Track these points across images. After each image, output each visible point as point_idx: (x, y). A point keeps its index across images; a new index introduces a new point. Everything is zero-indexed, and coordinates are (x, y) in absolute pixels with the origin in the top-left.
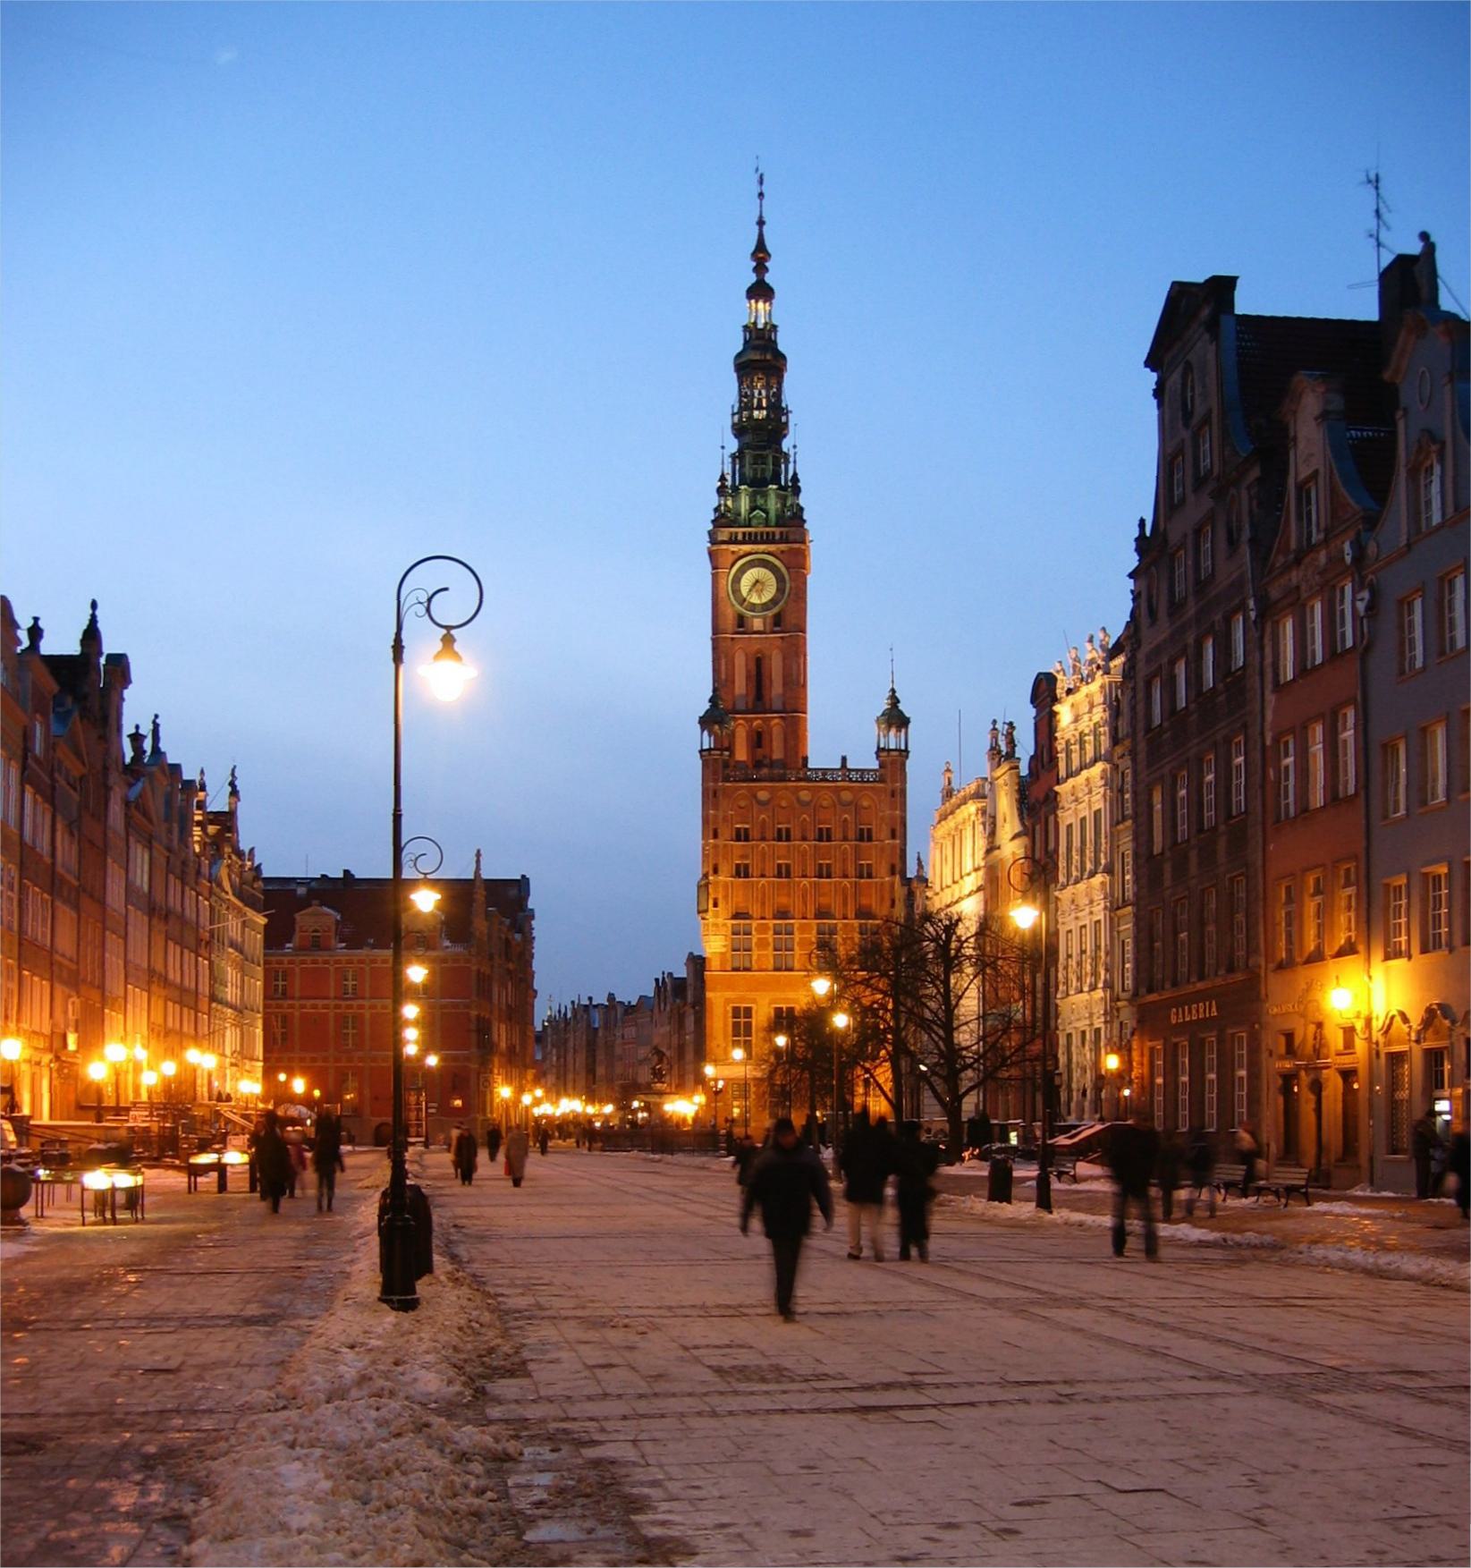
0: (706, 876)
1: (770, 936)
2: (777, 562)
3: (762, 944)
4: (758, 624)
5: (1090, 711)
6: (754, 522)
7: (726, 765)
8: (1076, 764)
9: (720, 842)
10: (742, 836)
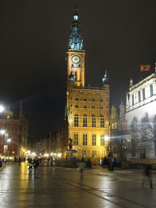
2: (79, 56)
3: (81, 121)
4: (75, 66)
9: (73, 100)
10: (77, 99)
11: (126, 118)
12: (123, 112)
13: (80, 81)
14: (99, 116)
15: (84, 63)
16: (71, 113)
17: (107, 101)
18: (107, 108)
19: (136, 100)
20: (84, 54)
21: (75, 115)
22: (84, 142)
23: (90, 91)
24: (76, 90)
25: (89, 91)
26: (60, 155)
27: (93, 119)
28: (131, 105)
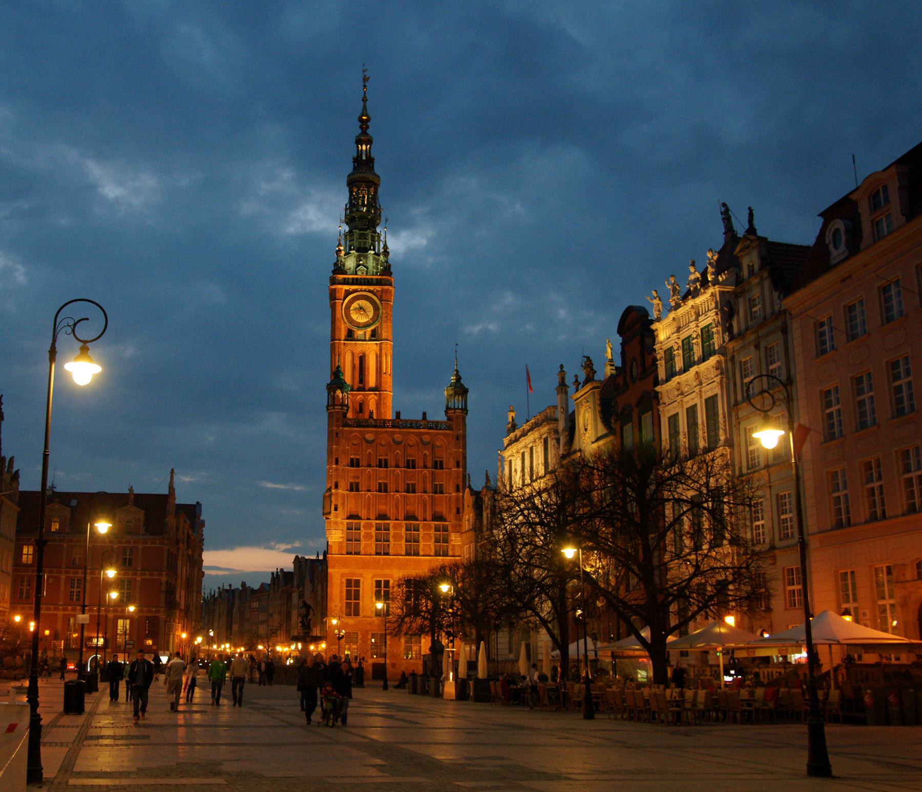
0: (330, 489)
1: (373, 531)
2: (374, 298)
4: (359, 333)
5: (697, 319)
6: (359, 273)
8: (679, 364)
9: (340, 467)
10: (354, 463)
14: (429, 517)
16: (336, 509)
17: (458, 466)
24: (353, 432)
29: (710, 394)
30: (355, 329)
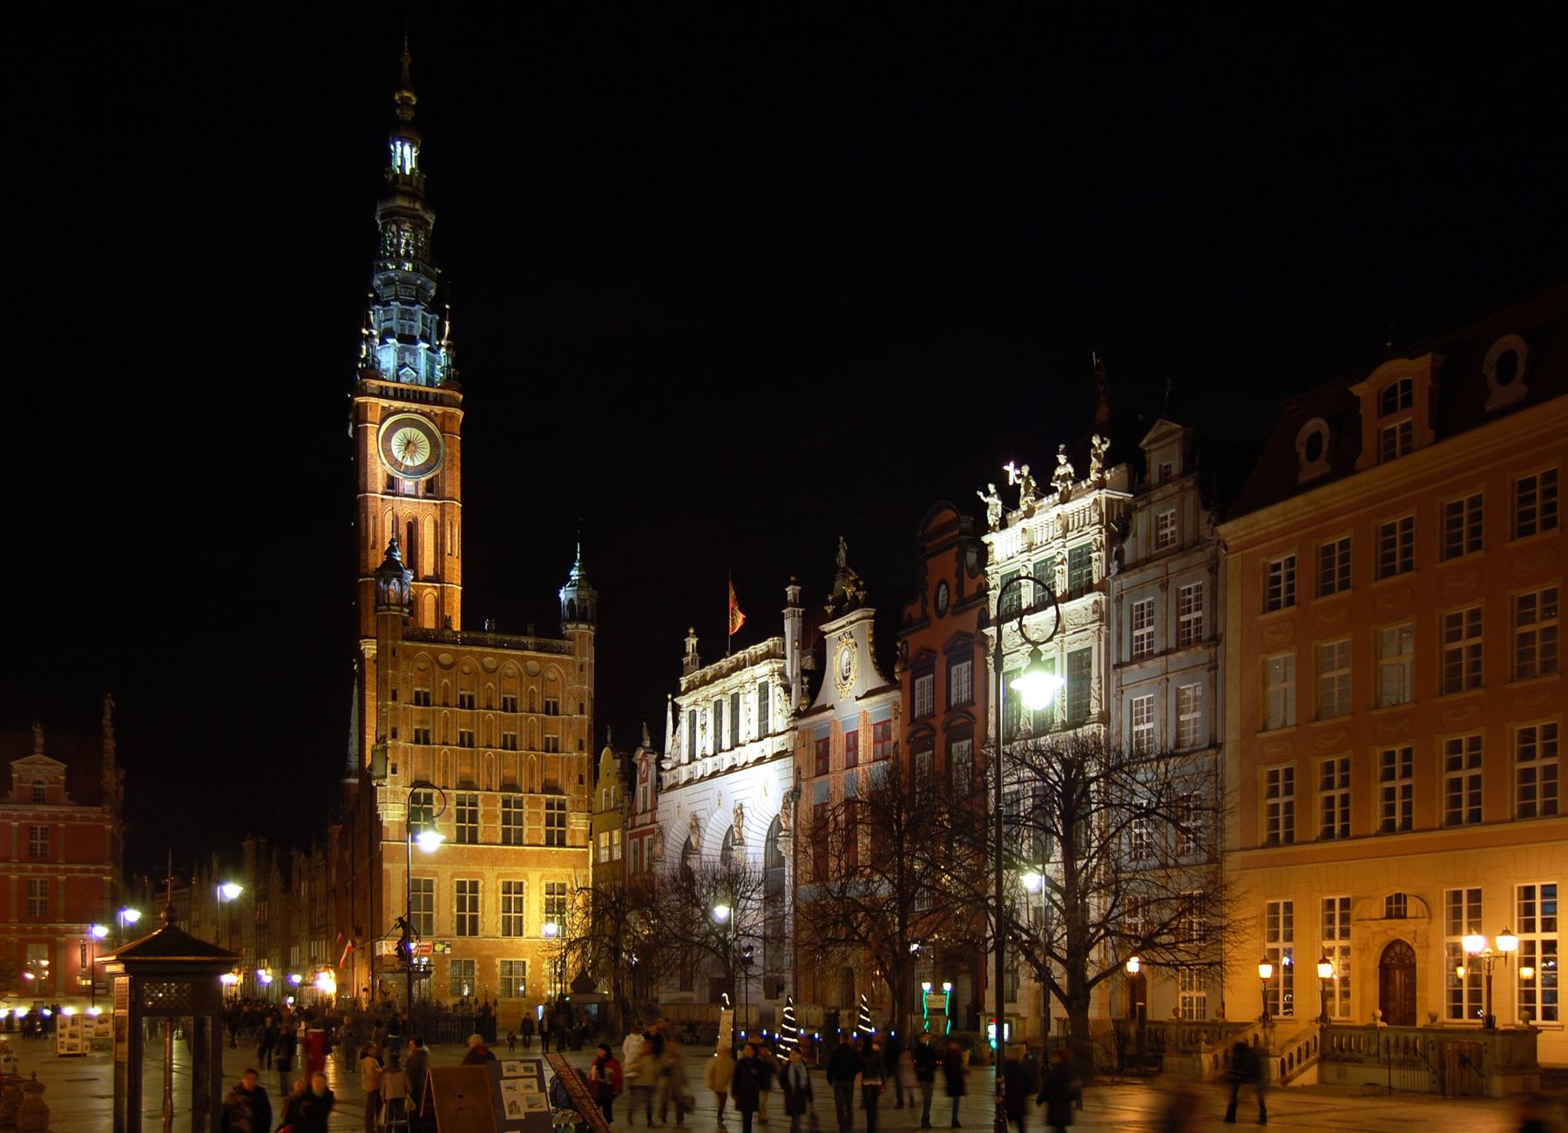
2: (431, 426)
4: (407, 485)
5: (1064, 536)
7: (405, 623)
9: (401, 704)
10: (422, 700)
11: (659, 817)
12: (649, 784)
13: (438, 577)
14: (538, 788)
15: (458, 474)
16: (394, 771)
17: (582, 712)
18: (581, 748)
19: (705, 742)
20: (460, 413)
21: (416, 784)
22: (461, 919)
23: (491, 656)
24: (418, 649)
25: (488, 655)
26: (327, 983)
27: (506, 803)
28: (685, 759)
29: (1077, 647)
30: (399, 476)
